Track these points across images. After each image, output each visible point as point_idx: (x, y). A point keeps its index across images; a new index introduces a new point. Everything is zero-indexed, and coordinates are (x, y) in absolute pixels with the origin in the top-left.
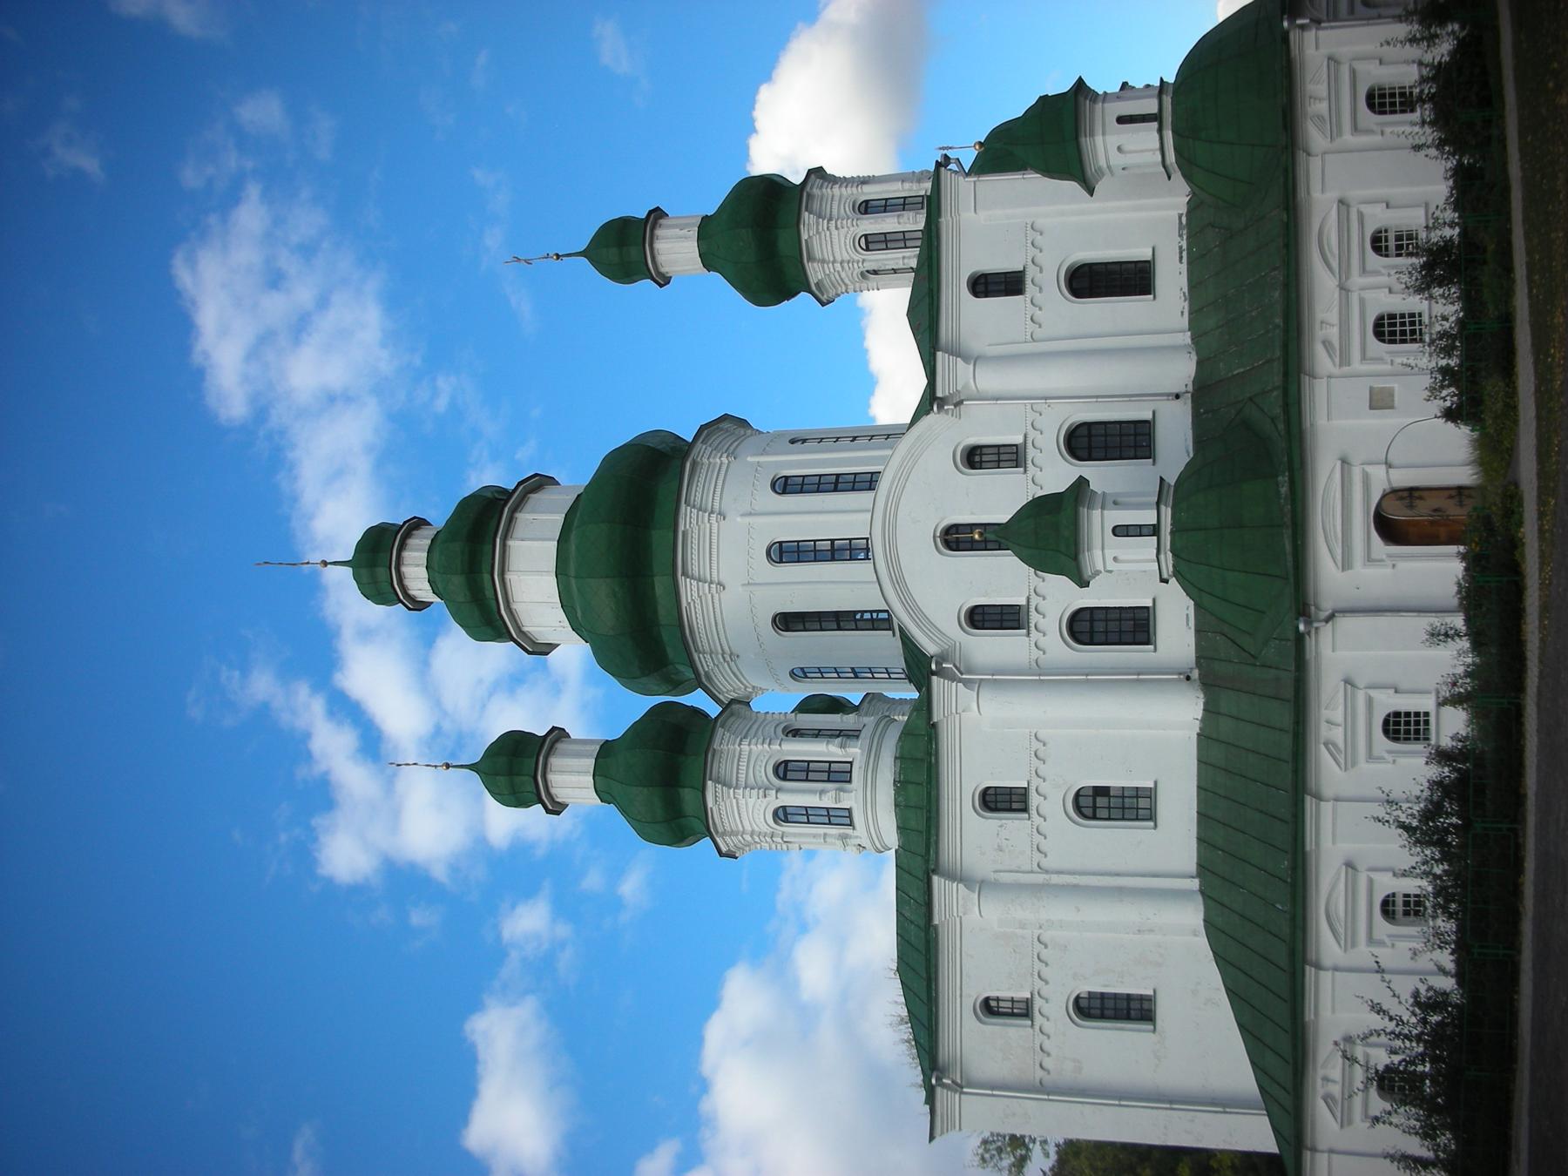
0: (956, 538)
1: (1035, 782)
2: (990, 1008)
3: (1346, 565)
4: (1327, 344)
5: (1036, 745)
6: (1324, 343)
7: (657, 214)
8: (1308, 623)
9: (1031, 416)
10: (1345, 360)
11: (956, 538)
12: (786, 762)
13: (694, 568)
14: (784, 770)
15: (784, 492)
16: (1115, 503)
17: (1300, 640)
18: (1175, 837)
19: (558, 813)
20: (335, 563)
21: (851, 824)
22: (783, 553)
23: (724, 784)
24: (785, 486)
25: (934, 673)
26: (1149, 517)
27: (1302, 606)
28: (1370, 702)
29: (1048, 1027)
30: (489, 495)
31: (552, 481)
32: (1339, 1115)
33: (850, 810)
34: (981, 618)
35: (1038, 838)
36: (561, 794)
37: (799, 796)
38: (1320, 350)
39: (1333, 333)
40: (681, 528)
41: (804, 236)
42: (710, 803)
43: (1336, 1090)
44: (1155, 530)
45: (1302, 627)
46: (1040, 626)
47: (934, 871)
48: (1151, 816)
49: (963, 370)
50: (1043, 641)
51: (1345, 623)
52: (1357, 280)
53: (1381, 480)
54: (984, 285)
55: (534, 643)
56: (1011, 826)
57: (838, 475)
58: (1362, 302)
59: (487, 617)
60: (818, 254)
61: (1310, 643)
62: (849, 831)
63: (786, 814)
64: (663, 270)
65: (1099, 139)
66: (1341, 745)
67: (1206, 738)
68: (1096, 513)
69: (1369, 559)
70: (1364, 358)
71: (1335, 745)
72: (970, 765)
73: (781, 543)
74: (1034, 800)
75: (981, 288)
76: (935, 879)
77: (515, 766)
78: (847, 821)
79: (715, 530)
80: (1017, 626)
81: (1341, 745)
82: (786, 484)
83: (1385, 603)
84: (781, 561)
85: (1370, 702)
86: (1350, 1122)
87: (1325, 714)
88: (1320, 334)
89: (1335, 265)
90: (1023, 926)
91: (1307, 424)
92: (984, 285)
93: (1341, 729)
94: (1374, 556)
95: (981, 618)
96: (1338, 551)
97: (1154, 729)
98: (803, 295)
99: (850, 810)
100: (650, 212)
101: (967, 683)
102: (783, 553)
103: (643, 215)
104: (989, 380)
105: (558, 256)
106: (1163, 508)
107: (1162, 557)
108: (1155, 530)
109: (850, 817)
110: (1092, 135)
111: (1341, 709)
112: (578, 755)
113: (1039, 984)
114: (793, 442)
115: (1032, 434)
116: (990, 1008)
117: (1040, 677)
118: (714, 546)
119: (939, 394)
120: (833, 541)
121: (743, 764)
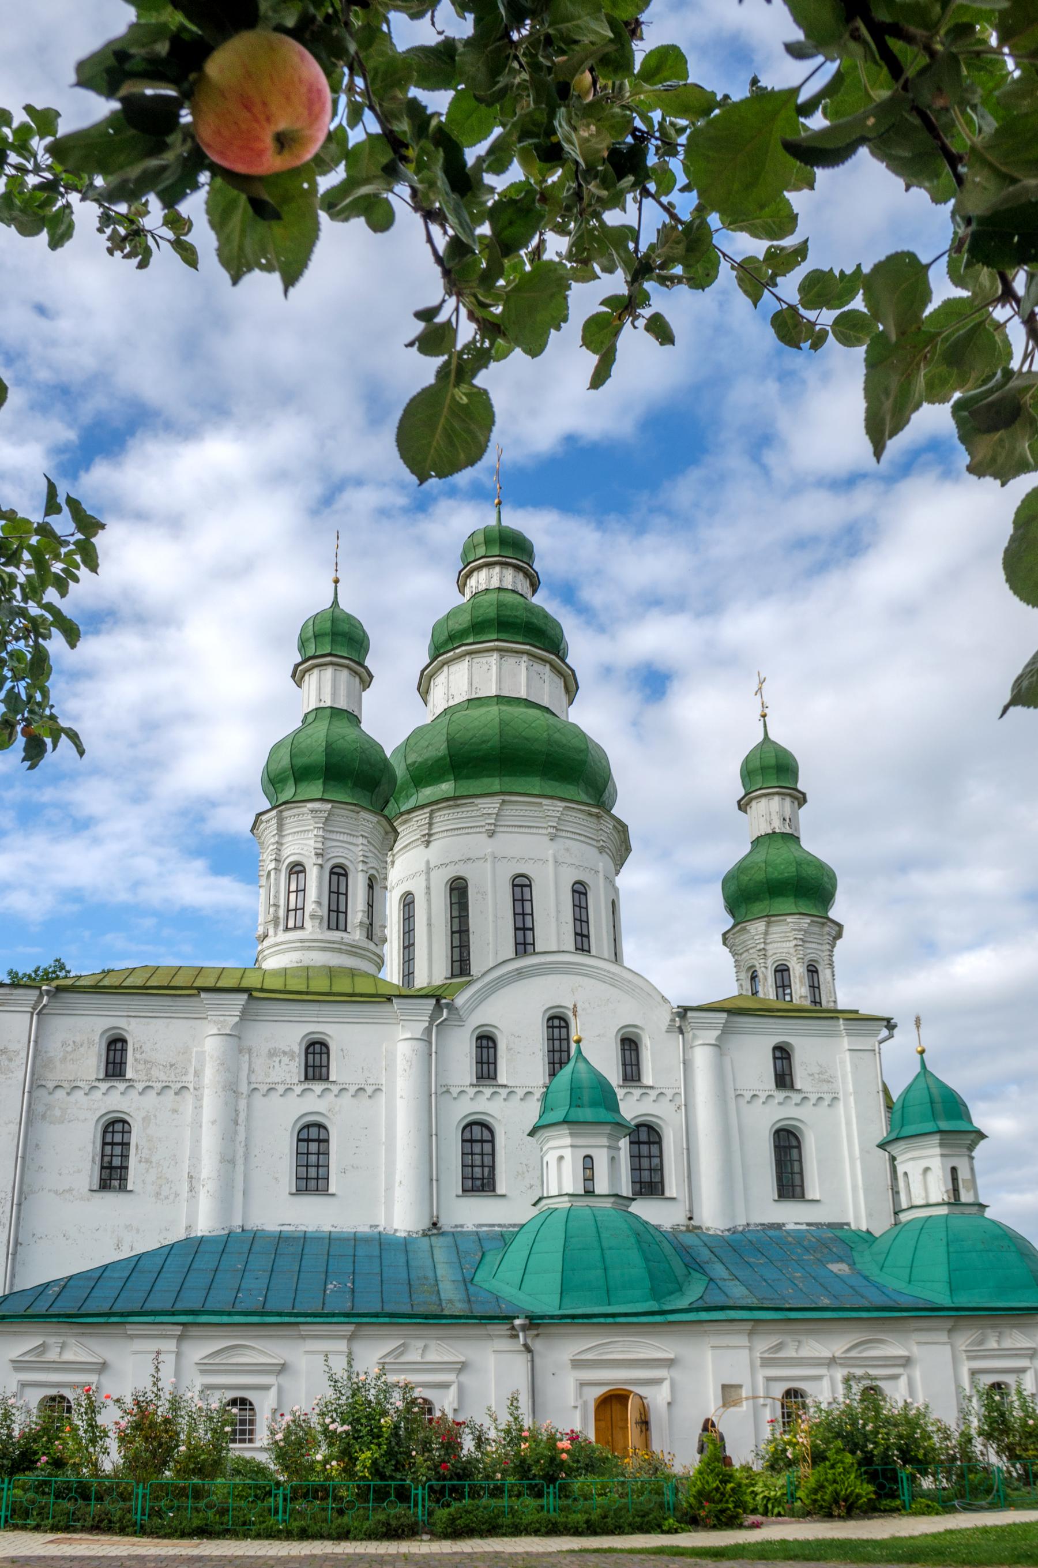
0: (558, 1024)
1: (335, 1089)
5: (370, 1090)
6: (781, 1343)
7: (801, 799)
8: (524, 1328)
9: (669, 1093)
10: (766, 1362)
11: (558, 1024)
12: (346, 875)
13: (508, 810)
14: (339, 873)
15: (574, 891)
16: (613, 1158)
19: (293, 676)
21: (287, 929)
22: (521, 887)
23: (327, 819)
24: (580, 891)
25: (438, 1001)
26: (602, 1186)
28: (445, 1386)
29: (97, 1094)
30: (562, 647)
31: (571, 703)
32: (26, 1358)
33: (302, 927)
34: (486, 1043)
35: (281, 1089)
36: (312, 680)
37: (314, 882)
38: (774, 1340)
39: (790, 1352)
40: (545, 801)
43: (52, 1355)
44: (589, 1193)
45: (517, 1322)
46: (480, 1096)
49: (711, 1036)
50: (465, 1099)
52: (839, 1374)
53: (658, 1397)
54: (782, 1054)
55: (431, 677)
56: (293, 1069)
57: (588, 937)
58: (819, 1378)
59: (449, 642)
60: (774, 929)
61: (503, 1329)
62: (281, 927)
63: (298, 873)
64: (754, 803)
66: (402, 1359)
68: (604, 1141)
69: (582, 1384)
70: (769, 1379)
71: (402, 1354)
73: (530, 886)
74: (318, 1087)
75: (778, 1054)
76: (245, 996)
77: (337, 642)
78: (291, 924)
79: (541, 831)
80: (480, 1077)
81: (402, 1359)
82: (580, 893)
83: (539, 1400)
84: (514, 886)
85: (445, 1386)
87: (433, 1344)
88: (788, 1339)
89: (853, 1354)
90: (197, 1074)
92: (782, 1054)
93: (419, 1359)
94: (586, 1389)
95: (486, 1043)
96: (589, 1356)
98: (731, 922)
99: (302, 927)
100: (804, 794)
101: (428, 1030)
102: (521, 887)
103: (800, 787)
104: (702, 1057)
105: (764, 716)
106: (612, 1200)
107: (566, 1198)
108: (589, 1193)
109: (295, 928)
111: (439, 1359)
112: (349, 695)
113: (140, 1086)
114: (613, 902)
115: (653, 1094)
117: (433, 1094)
118: (527, 830)
120: (532, 929)
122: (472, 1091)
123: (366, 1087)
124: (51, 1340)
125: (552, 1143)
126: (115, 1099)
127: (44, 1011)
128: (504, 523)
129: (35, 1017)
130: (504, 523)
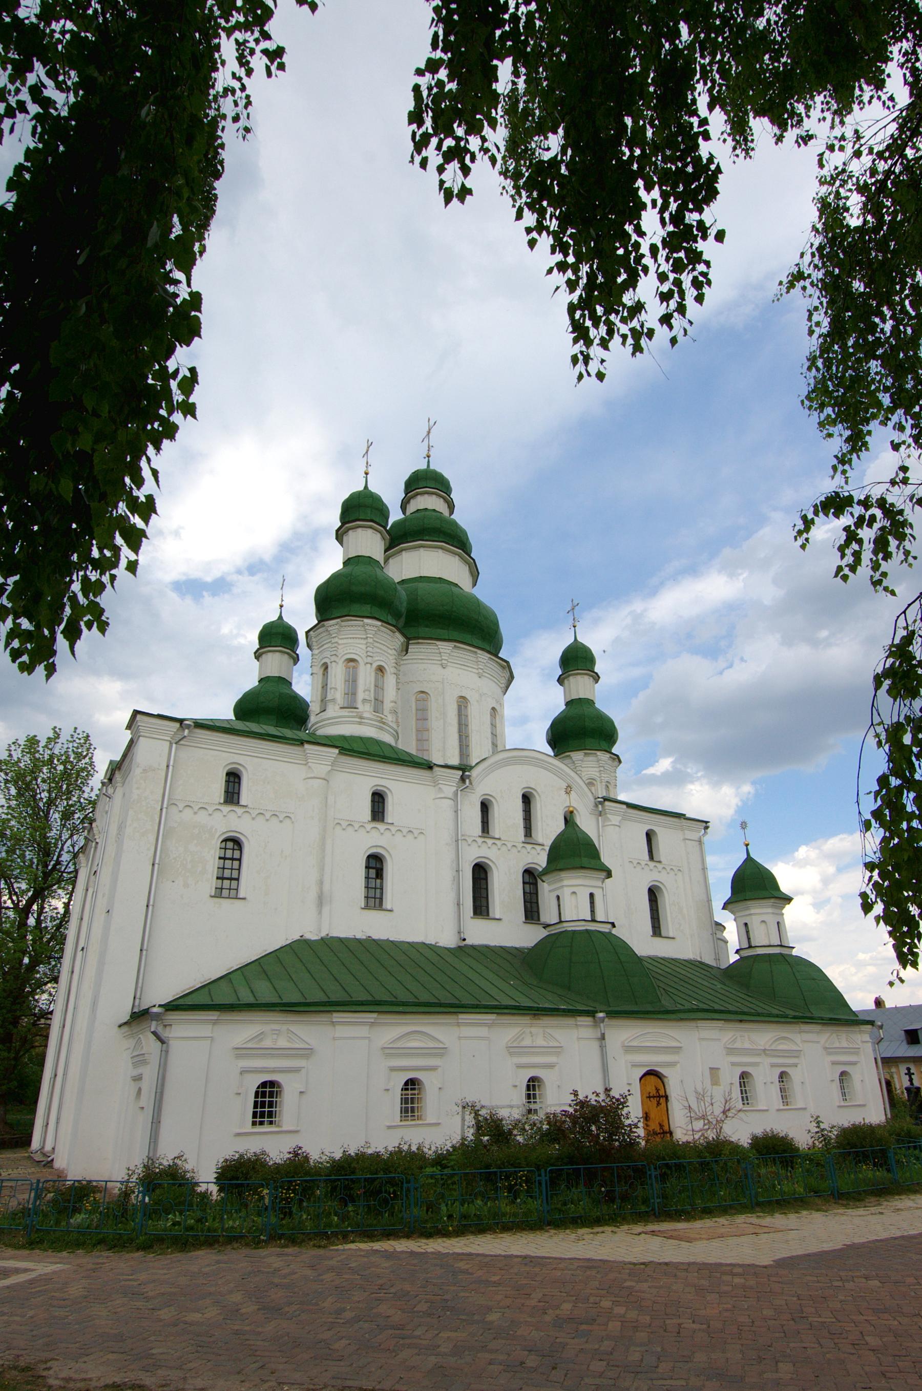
1: (393, 829)
2: (233, 778)
3: (628, 1049)
4: (734, 1041)
17: (591, 1013)
18: (351, 921)
20: (429, 462)
27: (613, 1014)
32: (249, 1045)
41: (599, 753)
42: (366, 621)
47: (340, 753)
48: (367, 907)
51: (595, 1045)
61: (588, 1020)
65: (770, 910)
67: (433, 948)
72: (402, 788)
74: (381, 826)
76: (337, 751)
86: (238, 1057)
91: (700, 1023)
97: (425, 913)
108: (593, 920)
110: (773, 906)
111: (544, 1044)
116: (233, 778)
119: (607, 803)
121: (384, 648)
122: (480, 840)
123: (414, 831)
124: (266, 1028)
125: (566, 883)
126: (231, 821)
127: (182, 742)
128: (432, 467)
129: (174, 745)
130: (432, 467)
